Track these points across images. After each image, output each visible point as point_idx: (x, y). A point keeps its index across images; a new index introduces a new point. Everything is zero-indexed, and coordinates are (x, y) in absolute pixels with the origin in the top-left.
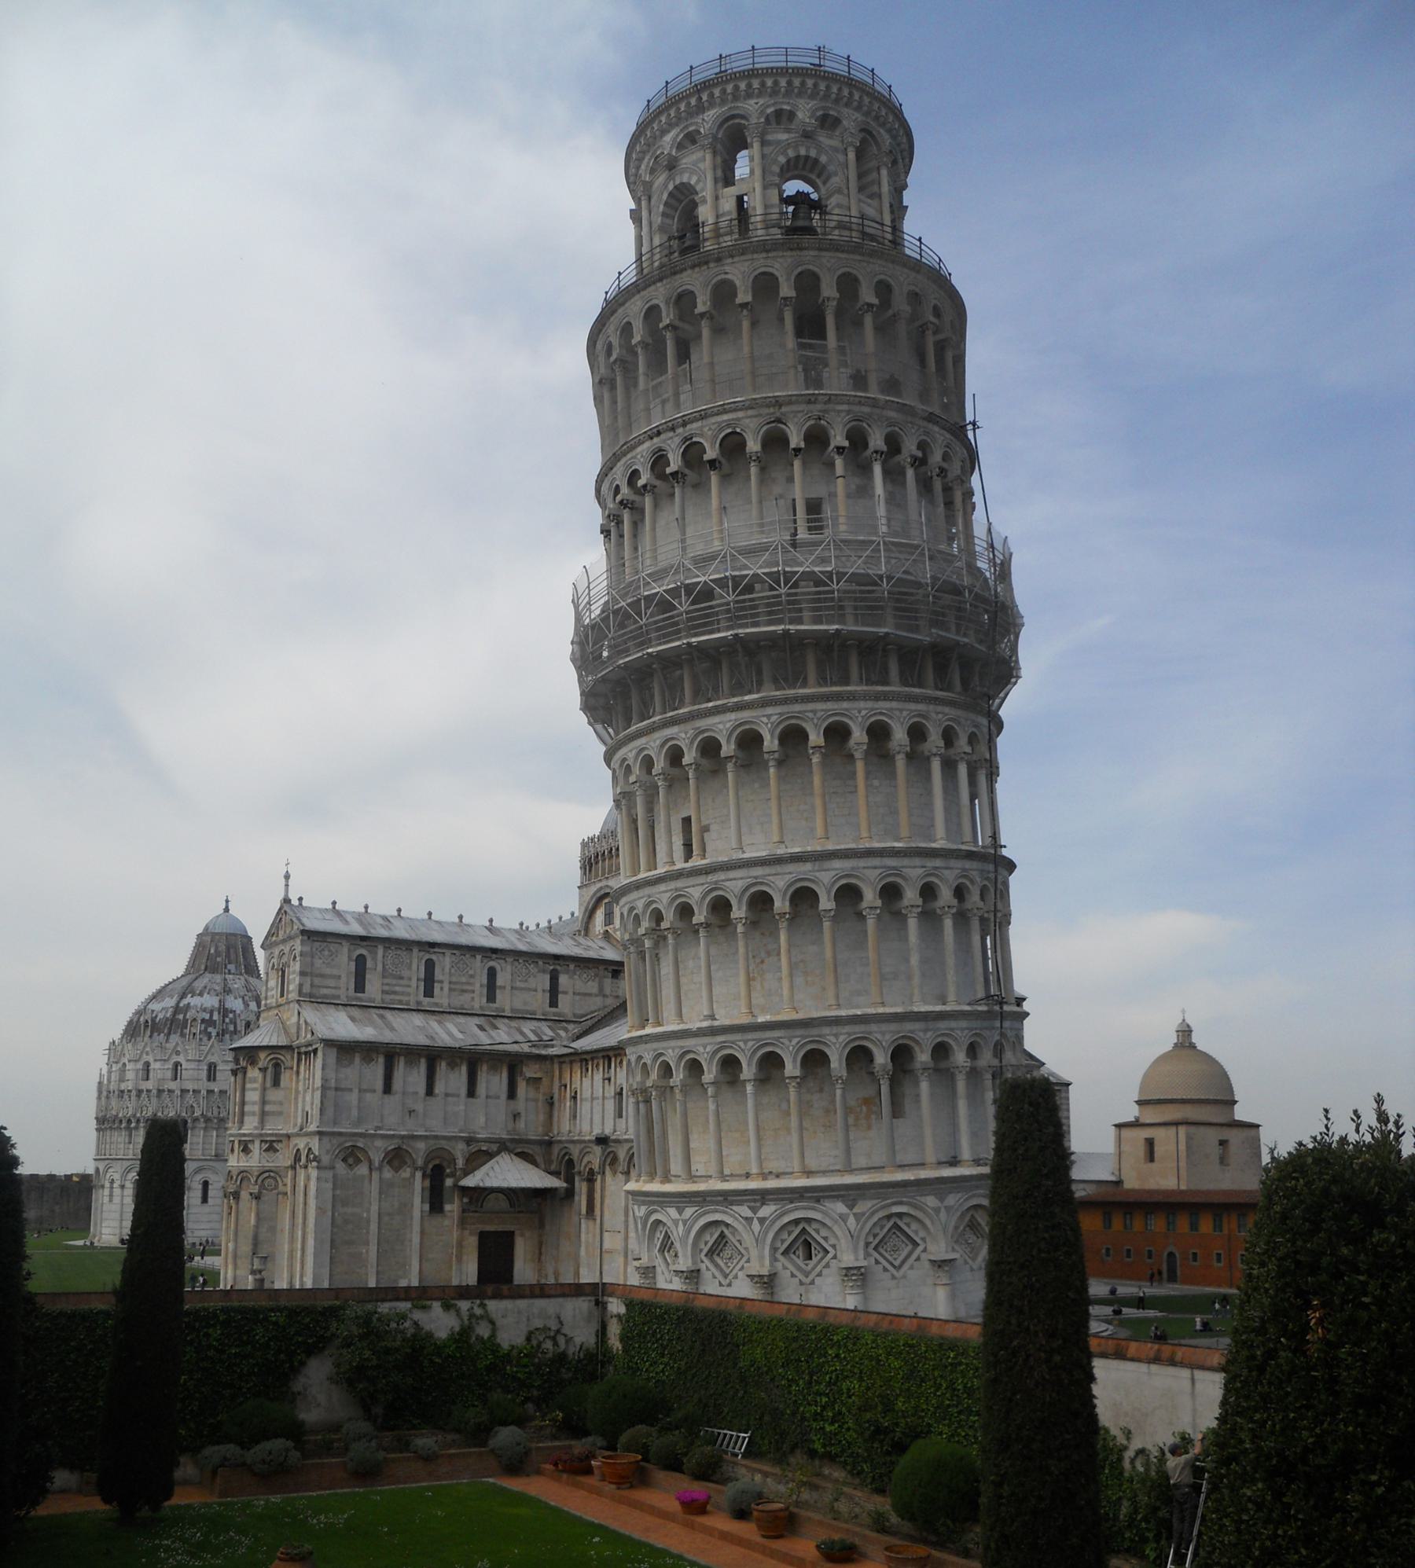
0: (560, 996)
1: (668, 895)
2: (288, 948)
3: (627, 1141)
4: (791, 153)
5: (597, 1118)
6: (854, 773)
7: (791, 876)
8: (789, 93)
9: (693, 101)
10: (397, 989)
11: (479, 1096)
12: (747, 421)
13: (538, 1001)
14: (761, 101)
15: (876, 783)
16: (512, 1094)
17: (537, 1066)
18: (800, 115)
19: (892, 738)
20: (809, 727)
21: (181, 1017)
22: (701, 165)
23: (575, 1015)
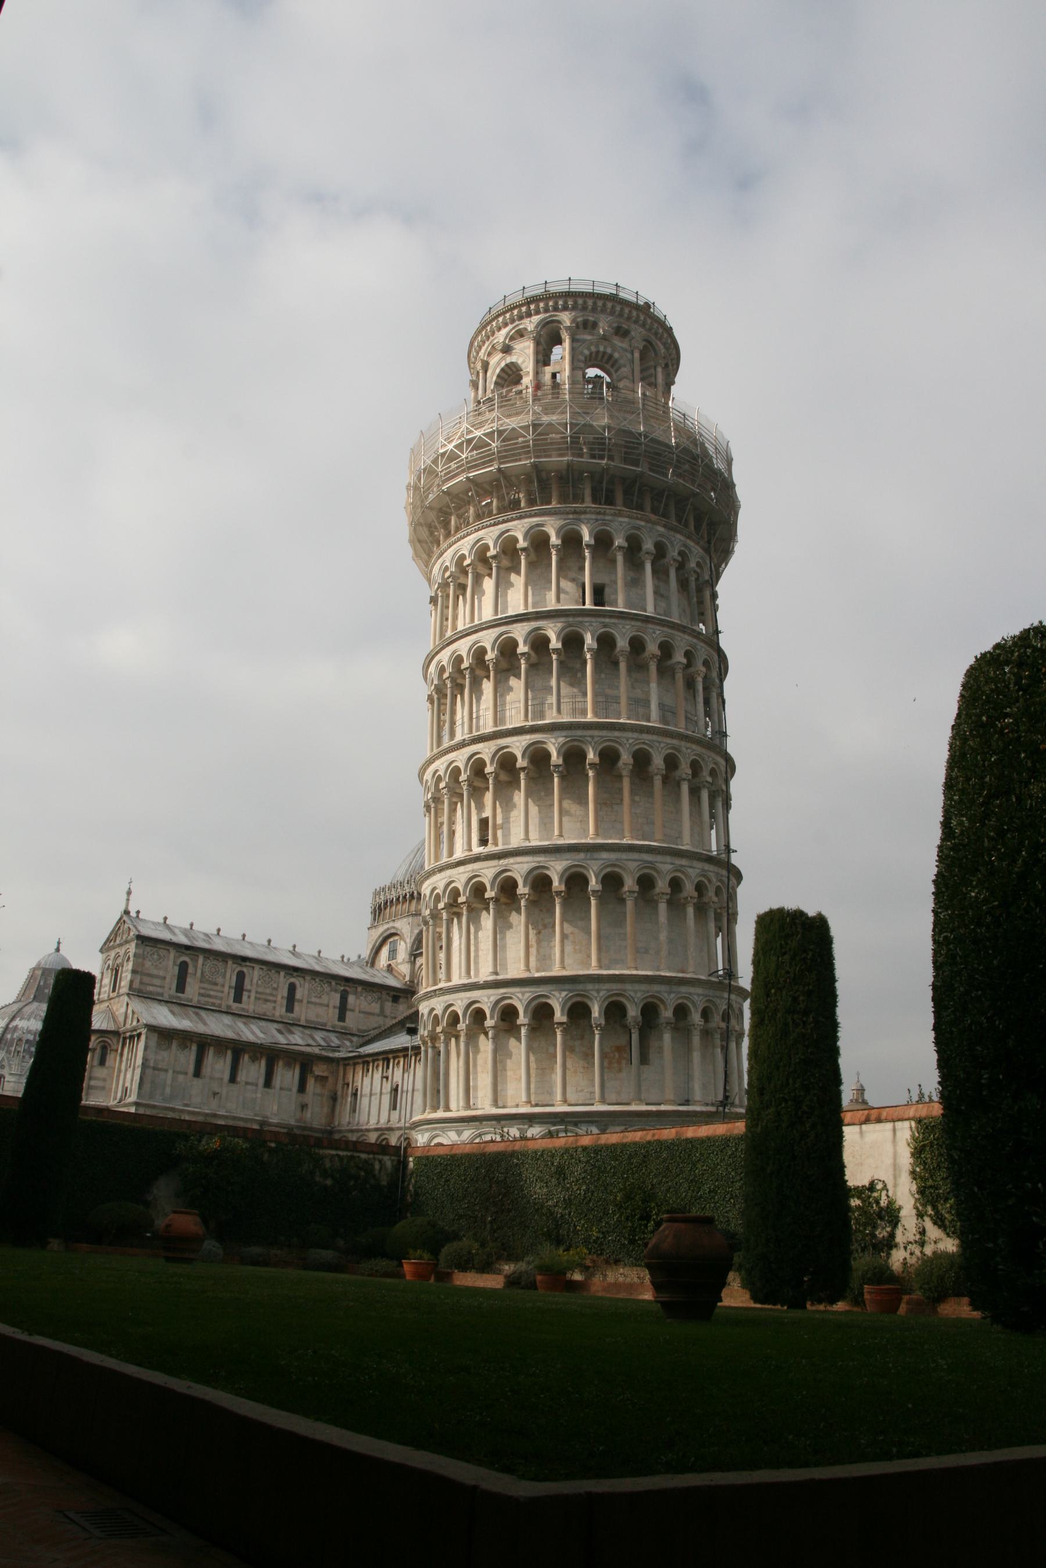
2: (123, 951)
3: (399, 1129)
6: (621, 790)
8: (594, 309)
9: (524, 309)
10: (212, 993)
11: (274, 1088)
13: (329, 1016)
15: (637, 798)
16: (302, 1088)
17: (325, 1066)
19: (652, 763)
22: (527, 351)
23: (359, 1030)
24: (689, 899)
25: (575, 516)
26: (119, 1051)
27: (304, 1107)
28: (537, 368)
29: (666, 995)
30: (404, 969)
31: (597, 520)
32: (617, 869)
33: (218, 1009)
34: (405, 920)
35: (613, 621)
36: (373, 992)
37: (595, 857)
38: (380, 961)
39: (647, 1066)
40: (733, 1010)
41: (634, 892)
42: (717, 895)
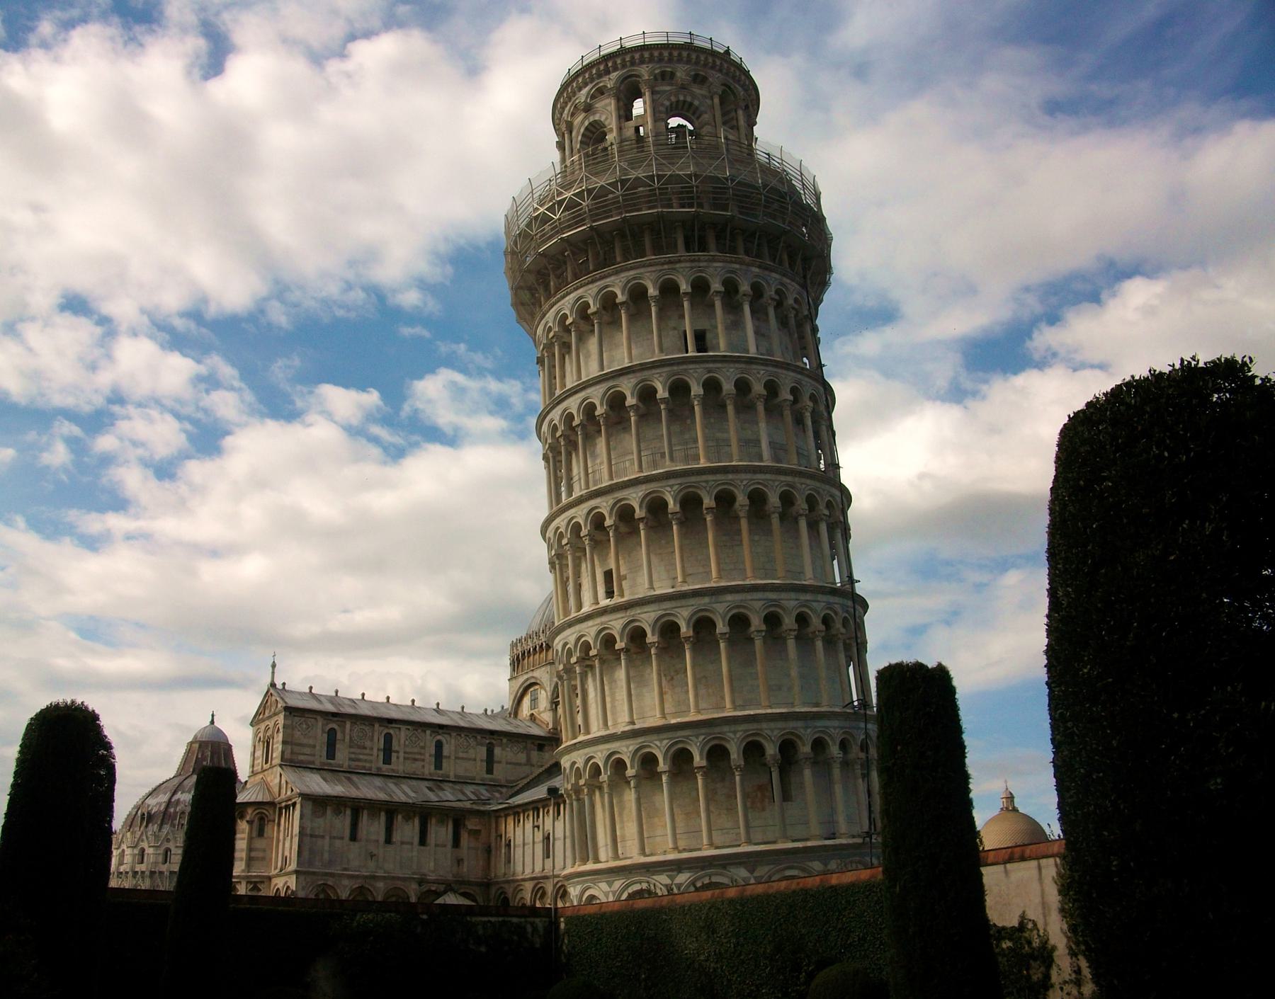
0: (495, 766)
5: (528, 859)
6: (740, 530)
7: (693, 608)
8: (670, 60)
9: (602, 67)
10: (361, 757)
12: (648, 274)
13: (478, 770)
14: (651, 66)
15: (756, 538)
16: (456, 843)
17: (477, 820)
18: (678, 74)
21: (172, 810)
22: (609, 108)
23: (507, 781)
24: (817, 632)
25: (671, 266)
26: (276, 821)
27: (459, 861)
28: (620, 123)
29: (802, 730)
30: (547, 717)
31: (692, 268)
32: (742, 610)
33: (368, 772)
34: (544, 669)
35: (719, 365)
36: (518, 742)
37: (720, 600)
38: (522, 711)
39: (790, 803)
40: (871, 739)
41: (762, 631)
42: (844, 626)
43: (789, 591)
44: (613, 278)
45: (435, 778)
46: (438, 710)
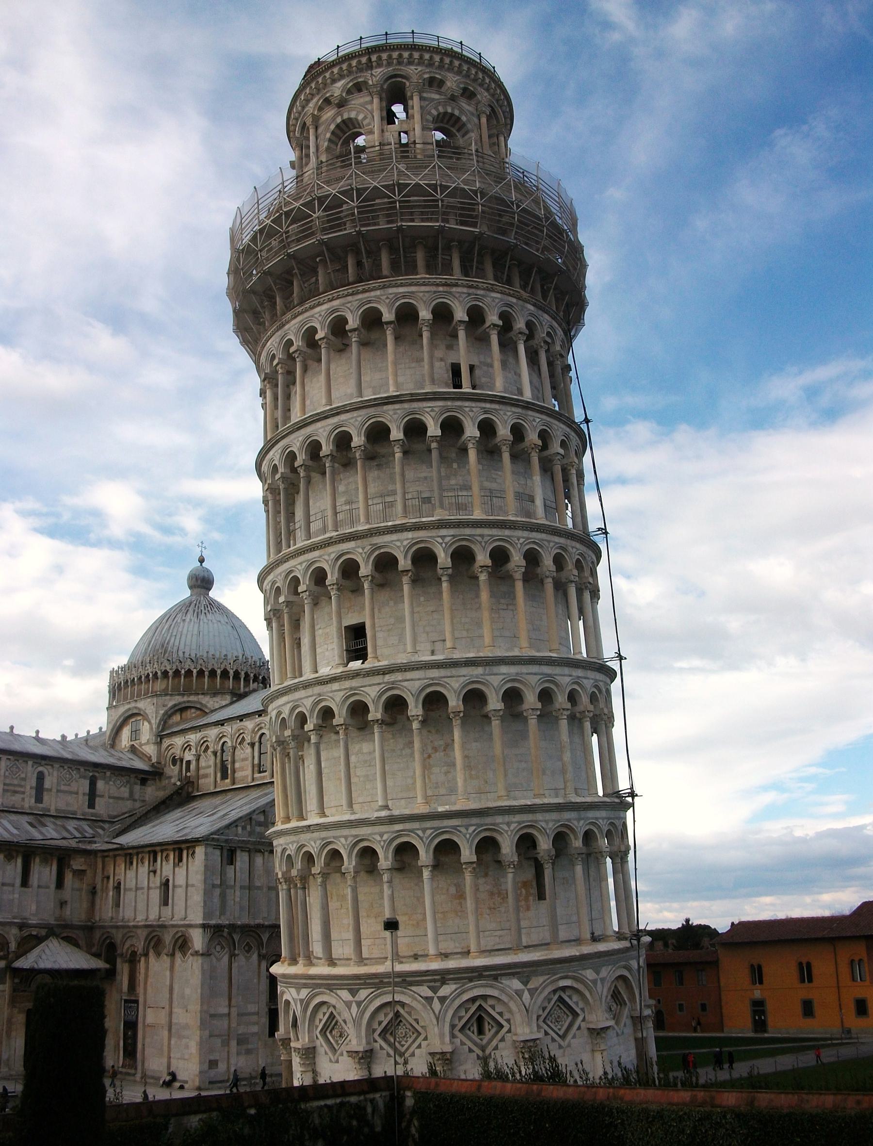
0: (97, 799)
1: (342, 693)
3: (173, 926)
4: (441, 109)
8: (441, 66)
9: (364, 60)
11: (32, 886)
12: (421, 294)
14: (420, 68)
16: (60, 884)
17: (83, 860)
18: (449, 84)
20: (476, 549)
23: (110, 816)
25: (446, 289)
27: (63, 904)
29: (575, 823)
30: (150, 750)
31: (469, 294)
34: (149, 700)
35: (496, 406)
36: (122, 776)
38: (121, 741)
43: (565, 666)
44: (378, 293)
45: (35, 812)
46: (37, 739)
